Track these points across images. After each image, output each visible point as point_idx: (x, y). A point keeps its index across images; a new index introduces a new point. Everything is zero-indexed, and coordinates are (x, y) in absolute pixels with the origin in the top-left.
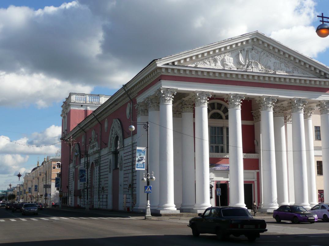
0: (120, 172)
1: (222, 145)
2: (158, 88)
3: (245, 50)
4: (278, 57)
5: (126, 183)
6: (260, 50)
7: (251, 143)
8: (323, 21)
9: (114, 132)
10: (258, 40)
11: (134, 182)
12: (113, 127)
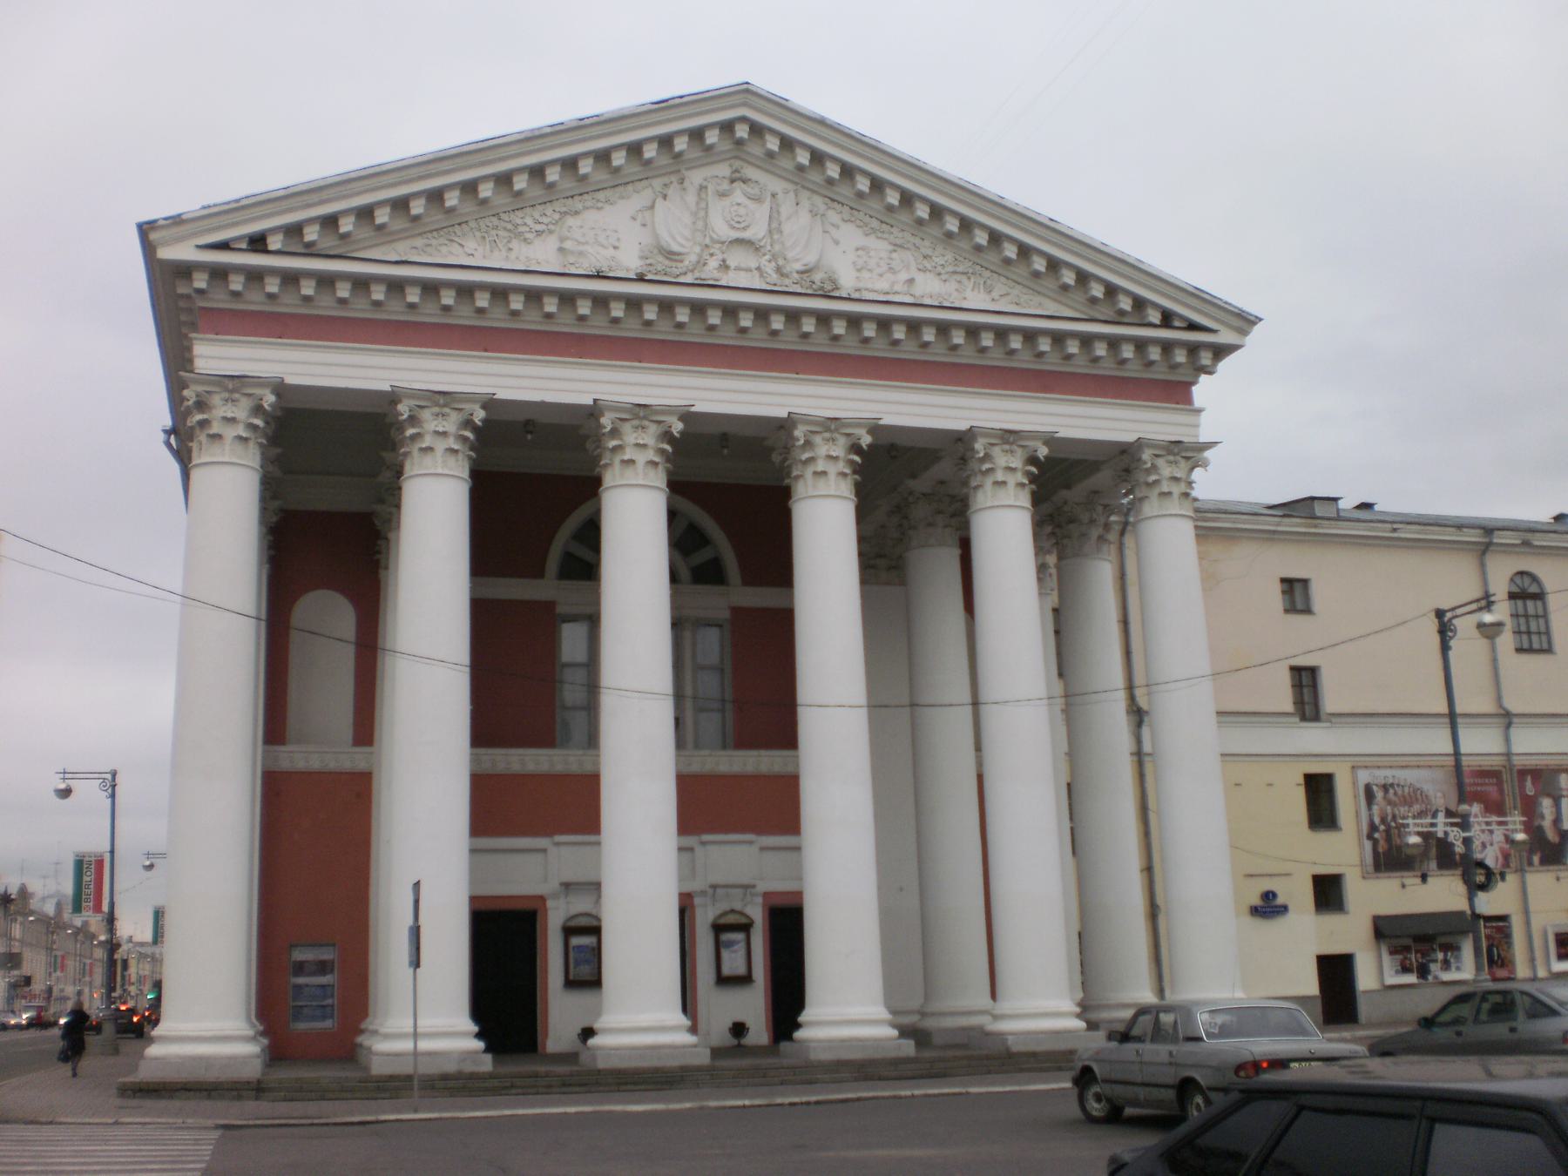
4: (875, 224)
6: (776, 185)
7: (744, 681)
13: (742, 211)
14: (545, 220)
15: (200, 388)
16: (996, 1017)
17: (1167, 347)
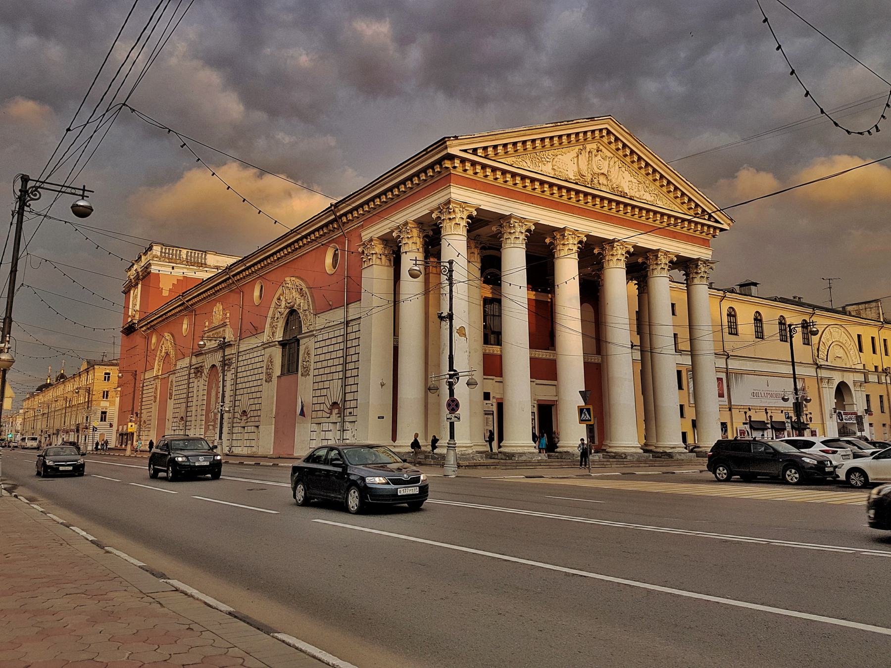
5: (321, 400)
6: (609, 154)
9: (283, 303)
10: (609, 132)
11: (349, 397)
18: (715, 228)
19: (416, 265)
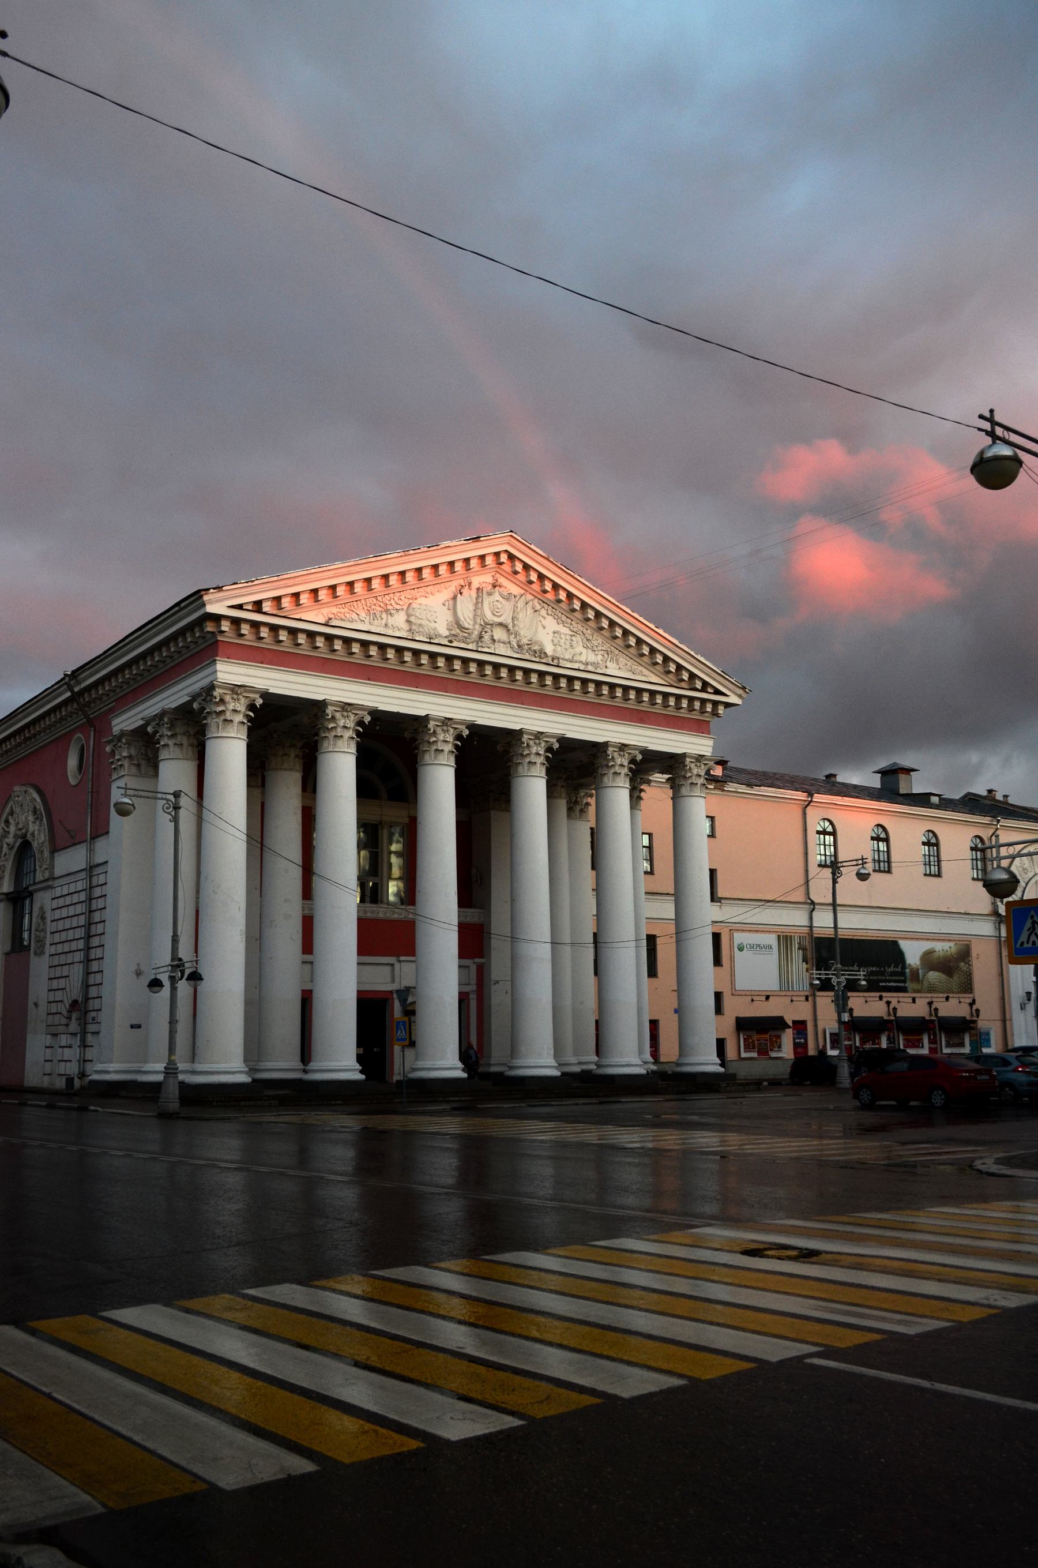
0: (34, 961)
1: (376, 880)
2: (205, 683)
3: (475, 584)
4: (564, 618)
5: (59, 996)
6: (515, 590)
8: (991, 434)
9: (12, 829)
10: (511, 557)
11: (93, 992)
12: (12, 813)
13: (499, 606)
14: (400, 602)
15: (222, 691)
16: (511, 1068)
17: (704, 701)
18: (715, 703)
19: (125, 796)
